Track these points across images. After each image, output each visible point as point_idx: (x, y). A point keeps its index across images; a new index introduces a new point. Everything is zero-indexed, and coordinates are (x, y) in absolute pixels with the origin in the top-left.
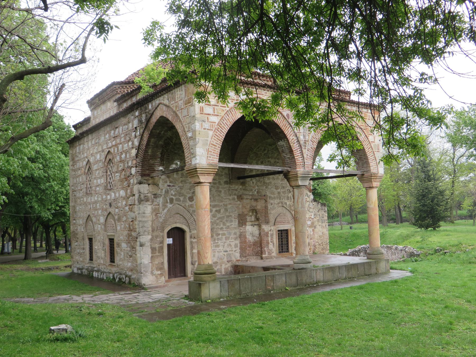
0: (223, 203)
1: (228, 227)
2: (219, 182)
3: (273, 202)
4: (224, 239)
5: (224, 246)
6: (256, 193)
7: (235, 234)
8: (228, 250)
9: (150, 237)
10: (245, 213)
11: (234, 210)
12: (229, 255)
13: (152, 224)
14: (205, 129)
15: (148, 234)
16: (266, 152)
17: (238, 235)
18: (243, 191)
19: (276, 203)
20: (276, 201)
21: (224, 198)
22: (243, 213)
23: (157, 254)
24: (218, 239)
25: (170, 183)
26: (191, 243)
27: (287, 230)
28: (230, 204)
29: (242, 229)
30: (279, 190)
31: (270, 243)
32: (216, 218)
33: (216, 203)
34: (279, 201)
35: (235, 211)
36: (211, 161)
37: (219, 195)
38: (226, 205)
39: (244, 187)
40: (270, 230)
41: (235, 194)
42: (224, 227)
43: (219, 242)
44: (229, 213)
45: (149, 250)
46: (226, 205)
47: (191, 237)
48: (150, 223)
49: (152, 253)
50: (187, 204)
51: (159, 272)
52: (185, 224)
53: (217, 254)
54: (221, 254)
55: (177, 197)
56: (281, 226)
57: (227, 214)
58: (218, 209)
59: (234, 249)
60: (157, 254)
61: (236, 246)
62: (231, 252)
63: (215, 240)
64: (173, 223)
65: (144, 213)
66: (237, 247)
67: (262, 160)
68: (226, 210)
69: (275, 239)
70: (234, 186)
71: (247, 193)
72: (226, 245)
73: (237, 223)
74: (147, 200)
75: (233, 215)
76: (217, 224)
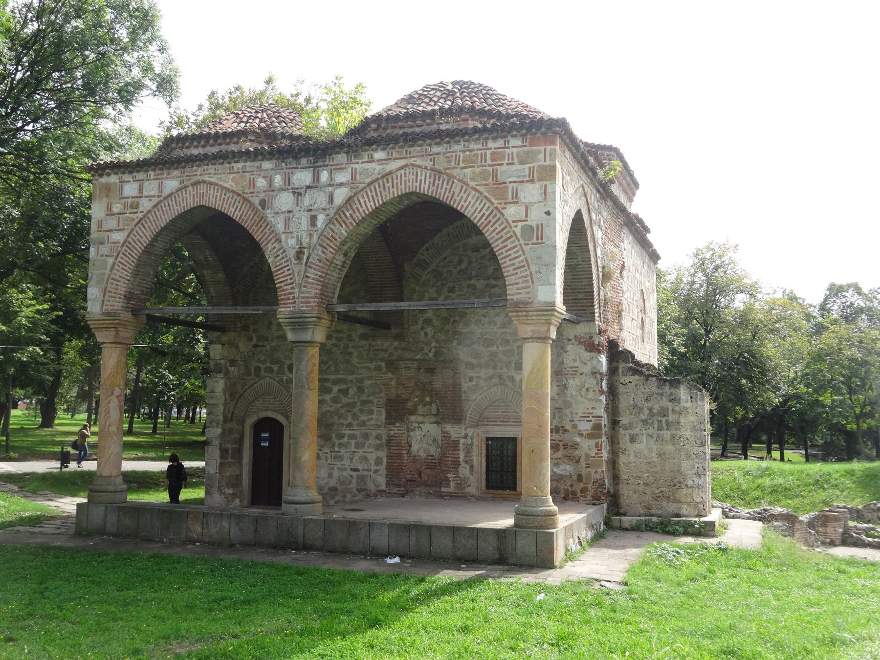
0: (355, 376)
1: (363, 423)
2: (349, 336)
3: (474, 375)
4: (353, 445)
5: (351, 459)
6: (431, 355)
7: (378, 437)
8: (360, 468)
9: (219, 431)
10: (404, 397)
11: (378, 390)
12: (362, 479)
13: (224, 409)
14: (102, 256)
15: (218, 427)
16: (464, 265)
17: (384, 441)
18: (400, 351)
19: (484, 377)
20: (483, 373)
21: (358, 366)
22: (398, 396)
23: (230, 460)
24: (340, 445)
25: (258, 340)
28: (371, 378)
29: (395, 430)
30: (494, 348)
31: (463, 464)
32: (339, 405)
33: (340, 377)
34: (490, 372)
35: (381, 391)
36: (110, 308)
37: (348, 361)
38: (361, 381)
39: (403, 345)
40: (466, 436)
41: (382, 360)
42: (355, 423)
43: (343, 451)
44: (368, 396)
46: (361, 381)
48: (221, 408)
49: (221, 458)
50: (285, 378)
51: (231, 491)
52: (281, 414)
53: (336, 473)
54: (345, 474)
55: (268, 364)
58: (343, 387)
59: (373, 468)
60: (230, 460)
61: (378, 461)
63: (333, 446)
64: (262, 411)
65: (213, 392)
66: (382, 464)
67: (451, 285)
68: (361, 390)
69: (479, 460)
70: (379, 342)
71: (408, 355)
72: (356, 458)
73: (383, 416)
75: (376, 401)
76: (340, 417)
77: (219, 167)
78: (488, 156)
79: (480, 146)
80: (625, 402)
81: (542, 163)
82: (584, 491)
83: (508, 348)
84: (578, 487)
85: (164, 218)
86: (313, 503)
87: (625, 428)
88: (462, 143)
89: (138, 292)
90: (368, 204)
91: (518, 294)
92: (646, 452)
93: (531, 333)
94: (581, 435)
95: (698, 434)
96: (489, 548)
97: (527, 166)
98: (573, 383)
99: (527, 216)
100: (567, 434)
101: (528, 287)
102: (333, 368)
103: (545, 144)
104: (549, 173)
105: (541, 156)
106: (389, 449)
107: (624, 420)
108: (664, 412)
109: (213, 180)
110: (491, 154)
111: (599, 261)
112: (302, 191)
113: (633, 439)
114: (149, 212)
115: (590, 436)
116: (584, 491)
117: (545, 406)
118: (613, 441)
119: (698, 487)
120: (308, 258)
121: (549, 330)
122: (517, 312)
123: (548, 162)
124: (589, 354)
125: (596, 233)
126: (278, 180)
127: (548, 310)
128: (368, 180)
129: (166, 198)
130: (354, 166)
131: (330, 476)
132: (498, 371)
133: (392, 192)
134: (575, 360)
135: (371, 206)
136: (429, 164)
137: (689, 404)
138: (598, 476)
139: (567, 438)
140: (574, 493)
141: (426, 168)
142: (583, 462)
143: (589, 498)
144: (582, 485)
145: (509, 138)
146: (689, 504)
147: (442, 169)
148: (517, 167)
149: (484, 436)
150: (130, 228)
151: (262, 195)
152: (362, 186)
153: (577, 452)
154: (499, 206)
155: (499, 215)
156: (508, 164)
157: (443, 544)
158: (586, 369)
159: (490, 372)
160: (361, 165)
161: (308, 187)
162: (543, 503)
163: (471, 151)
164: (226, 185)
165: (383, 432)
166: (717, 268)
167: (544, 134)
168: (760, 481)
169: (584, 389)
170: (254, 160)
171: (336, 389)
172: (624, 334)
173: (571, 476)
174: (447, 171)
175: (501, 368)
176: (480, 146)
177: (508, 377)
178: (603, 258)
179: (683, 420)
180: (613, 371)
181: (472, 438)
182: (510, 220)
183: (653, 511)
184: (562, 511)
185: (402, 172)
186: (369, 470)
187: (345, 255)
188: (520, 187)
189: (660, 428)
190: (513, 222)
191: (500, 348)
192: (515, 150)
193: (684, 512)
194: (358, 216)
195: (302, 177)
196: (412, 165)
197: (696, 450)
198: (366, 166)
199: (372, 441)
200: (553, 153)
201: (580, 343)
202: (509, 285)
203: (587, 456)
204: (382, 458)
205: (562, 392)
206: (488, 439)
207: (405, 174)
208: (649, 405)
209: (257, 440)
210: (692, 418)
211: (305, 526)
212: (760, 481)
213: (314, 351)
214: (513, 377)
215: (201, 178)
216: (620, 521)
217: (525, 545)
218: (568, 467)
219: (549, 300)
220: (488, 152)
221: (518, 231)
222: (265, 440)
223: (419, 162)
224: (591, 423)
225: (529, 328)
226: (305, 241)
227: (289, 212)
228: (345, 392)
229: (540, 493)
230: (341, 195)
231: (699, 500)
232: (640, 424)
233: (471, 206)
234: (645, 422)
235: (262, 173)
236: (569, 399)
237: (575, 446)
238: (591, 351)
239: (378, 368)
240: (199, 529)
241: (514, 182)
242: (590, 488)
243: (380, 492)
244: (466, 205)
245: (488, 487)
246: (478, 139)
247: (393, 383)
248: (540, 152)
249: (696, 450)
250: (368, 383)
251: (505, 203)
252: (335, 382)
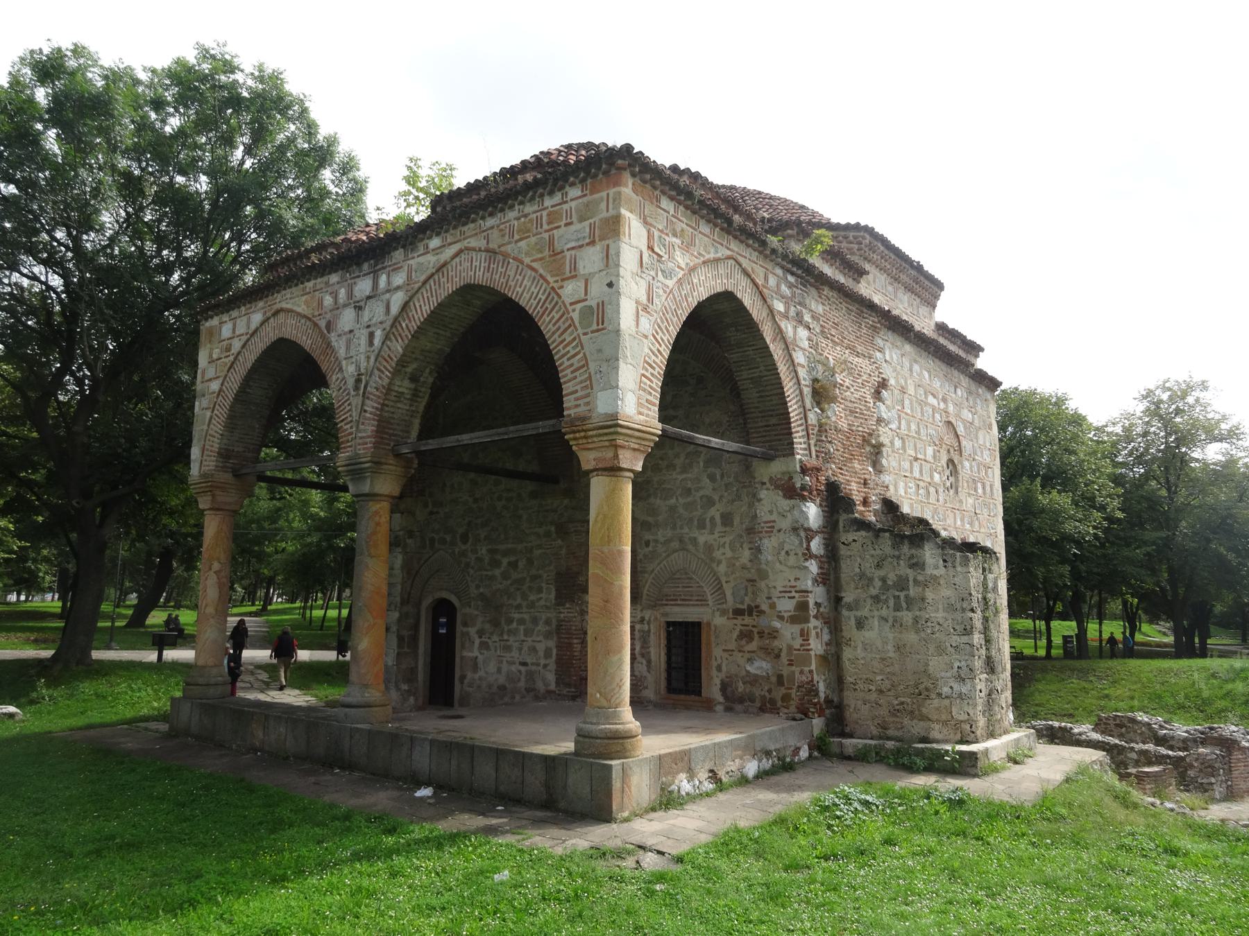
3: (651, 538)
5: (520, 649)
7: (548, 622)
8: (529, 661)
9: (397, 615)
12: (531, 676)
19: (662, 540)
24: (510, 632)
27: (698, 625)
28: (539, 547)
29: (567, 612)
30: (673, 501)
33: (510, 546)
42: (524, 604)
43: (512, 639)
48: (399, 587)
49: (399, 646)
50: (457, 550)
53: (505, 667)
54: (513, 668)
56: (676, 609)
57: (533, 572)
58: (512, 559)
59: (542, 662)
60: (406, 650)
61: (548, 654)
62: (534, 668)
63: (502, 634)
66: (551, 656)
68: (530, 562)
72: (525, 648)
73: (553, 596)
77: (294, 289)
78: (544, 219)
79: (536, 208)
80: (848, 569)
81: (604, 215)
82: (786, 698)
83: (689, 499)
84: (778, 693)
85: (250, 357)
86: (370, 707)
87: (850, 608)
88: (517, 207)
89: (241, 449)
90: (423, 308)
91: (577, 406)
92: (879, 644)
93: (594, 463)
94: (781, 618)
95: (958, 616)
96: (535, 782)
97: (587, 223)
98: (769, 544)
99: (586, 294)
100: (762, 617)
101: (588, 395)
102: (502, 536)
103: (608, 188)
104: (613, 227)
105: (603, 206)
106: (559, 638)
107: (848, 597)
108: (902, 584)
109: (289, 306)
110: (548, 215)
111: (802, 373)
112: (362, 304)
113: (860, 624)
114: (239, 353)
115: (794, 620)
116: (786, 698)
117: (618, 571)
118: (834, 625)
119: (961, 696)
120: (365, 387)
121: (616, 456)
122: (574, 432)
123: (612, 212)
124: (788, 501)
125: (783, 326)
126: (342, 293)
127: (610, 427)
128: (423, 278)
129: (252, 335)
130: (411, 262)
131: (499, 670)
132: (678, 531)
133: (447, 287)
134: (771, 512)
135: (426, 310)
136: (482, 243)
137: (941, 571)
138: (804, 678)
139: (763, 622)
140: (773, 702)
141: (480, 250)
142: (784, 659)
143: (793, 709)
144: (783, 691)
145: (567, 188)
146: (945, 723)
147: (496, 247)
148: (576, 226)
149: (663, 620)
150: (223, 374)
151: (328, 316)
152: (417, 286)
153: (776, 643)
154: (555, 285)
155: (556, 298)
156: (566, 225)
157: (485, 771)
158: (785, 524)
159: (669, 533)
160: (417, 260)
161: (369, 298)
162: (607, 718)
163: (526, 216)
164: (299, 310)
166: (1178, 412)
167: (606, 173)
168: (1230, 686)
169: (783, 553)
170: (322, 276)
171: (505, 561)
172: (887, 478)
173: (768, 678)
174: (502, 249)
175: (681, 528)
176: (536, 208)
177: (690, 539)
178: (811, 370)
179: (929, 595)
180: (831, 526)
181: (649, 623)
182: (568, 301)
183: (891, 732)
184: (648, 729)
185: (457, 260)
186: (538, 665)
187: (414, 379)
188: (578, 253)
189: (897, 608)
190: (571, 304)
191: (681, 501)
192: (573, 204)
193: (935, 734)
194: (414, 326)
195: (363, 286)
196: (467, 249)
197: (956, 640)
198: (421, 259)
199: (541, 627)
200: (618, 199)
201: (777, 487)
202: (568, 395)
203: (790, 648)
204: (551, 649)
205: (756, 557)
206: (669, 624)
207: (459, 261)
208: (882, 573)
209: (435, 625)
210: (946, 592)
211: (351, 737)
212: (1230, 686)
213: (383, 507)
214: (695, 539)
215: (278, 306)
216: (841, 744)
217: (577, 783)
218: (764, 664)
219: (610, 410)
220: (545, 213)
221: (576, 316)
222: (443, 625)
223: (473, 243)
224: (794, 602)
225: (592, 455)
226: (363, 365)
227: (351, 331)
228: (514, 565)
229: (605, 703)
230: (397, 300)
231: (963, 717)
232: (869, 601)
233: (526, 293)
234: (876, 599)
235: (330, 289)
236: (764, 566)
237: (774, 634)
238: (791, 498)
239: (548, 534)
240: (260, 734)
241: (573, 248)
242: (793, 696)
243: (549, 692)
244: (520, 290)
245: (671, 689)
246: (532, 199)
247: (564, 551)
248: (602, 199)
249: (956, 640)
250: (537, 552)
251: (563, 280)
252: (506, 553)
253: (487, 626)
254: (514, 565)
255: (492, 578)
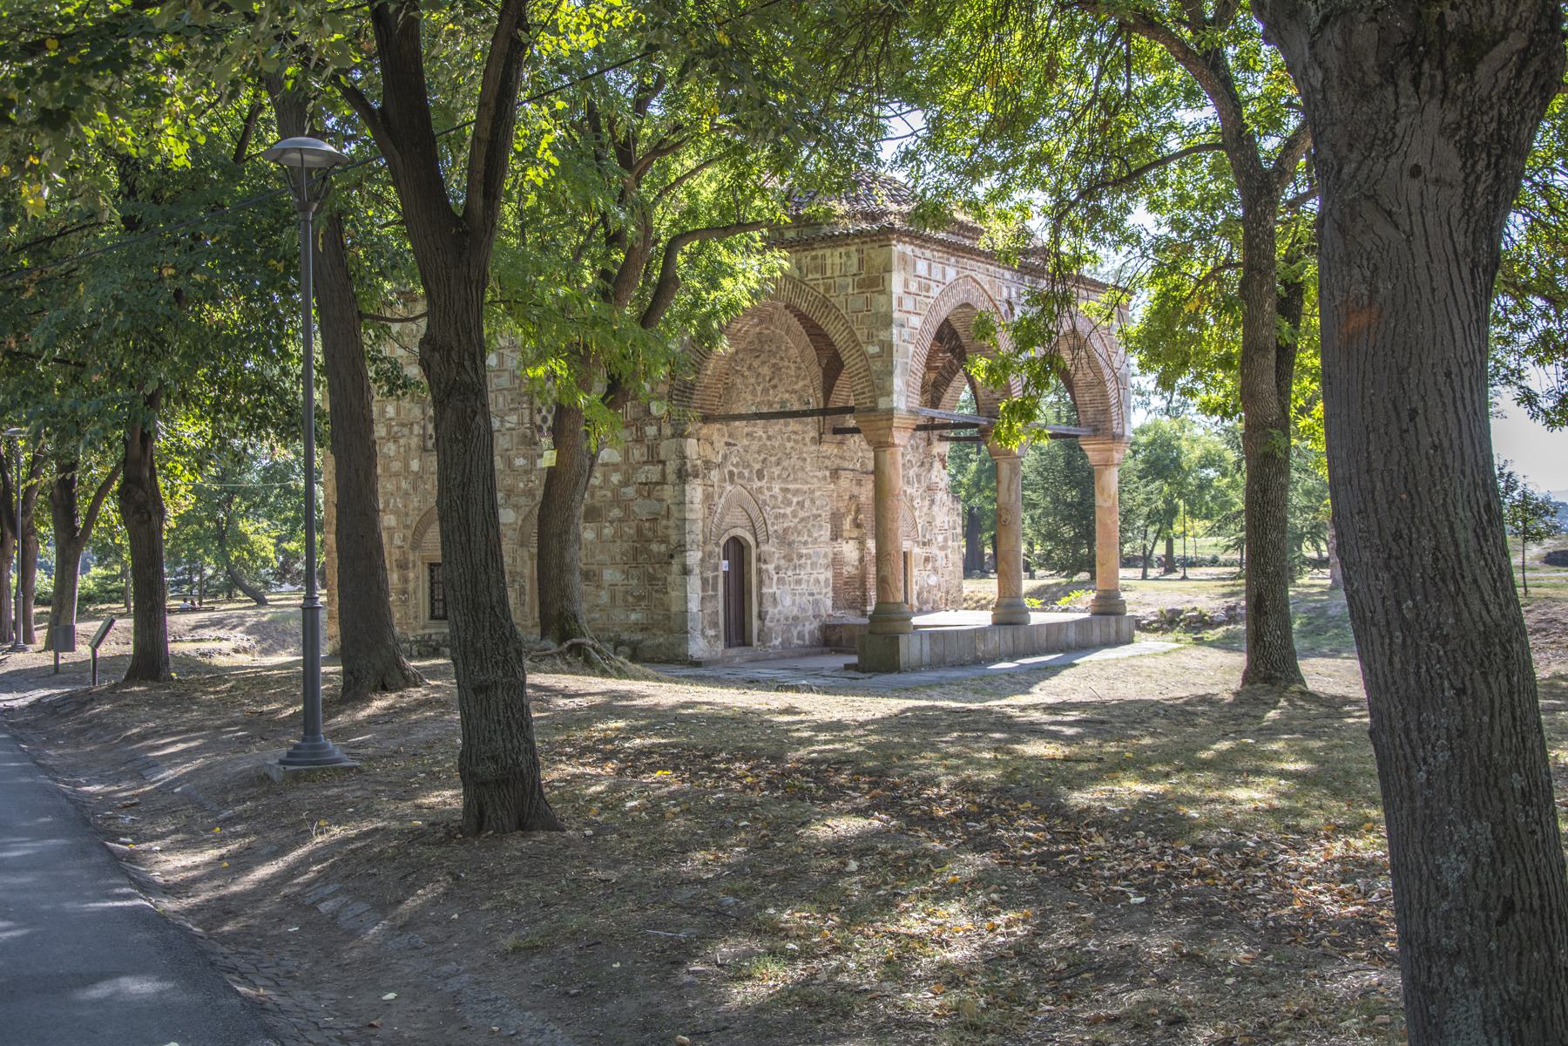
9: (699, 555)
26: (759, 571)
45: (699, 582)
46: (812, 492)
47: (759, 559)
49: (704, 590)
68: (813, 501)
74: (696, 476)
165: (829, 550)
228: (801, 504)
252: (796, 492)
253: (782, 562)
254: (801, 504)
255: (784, 516)
